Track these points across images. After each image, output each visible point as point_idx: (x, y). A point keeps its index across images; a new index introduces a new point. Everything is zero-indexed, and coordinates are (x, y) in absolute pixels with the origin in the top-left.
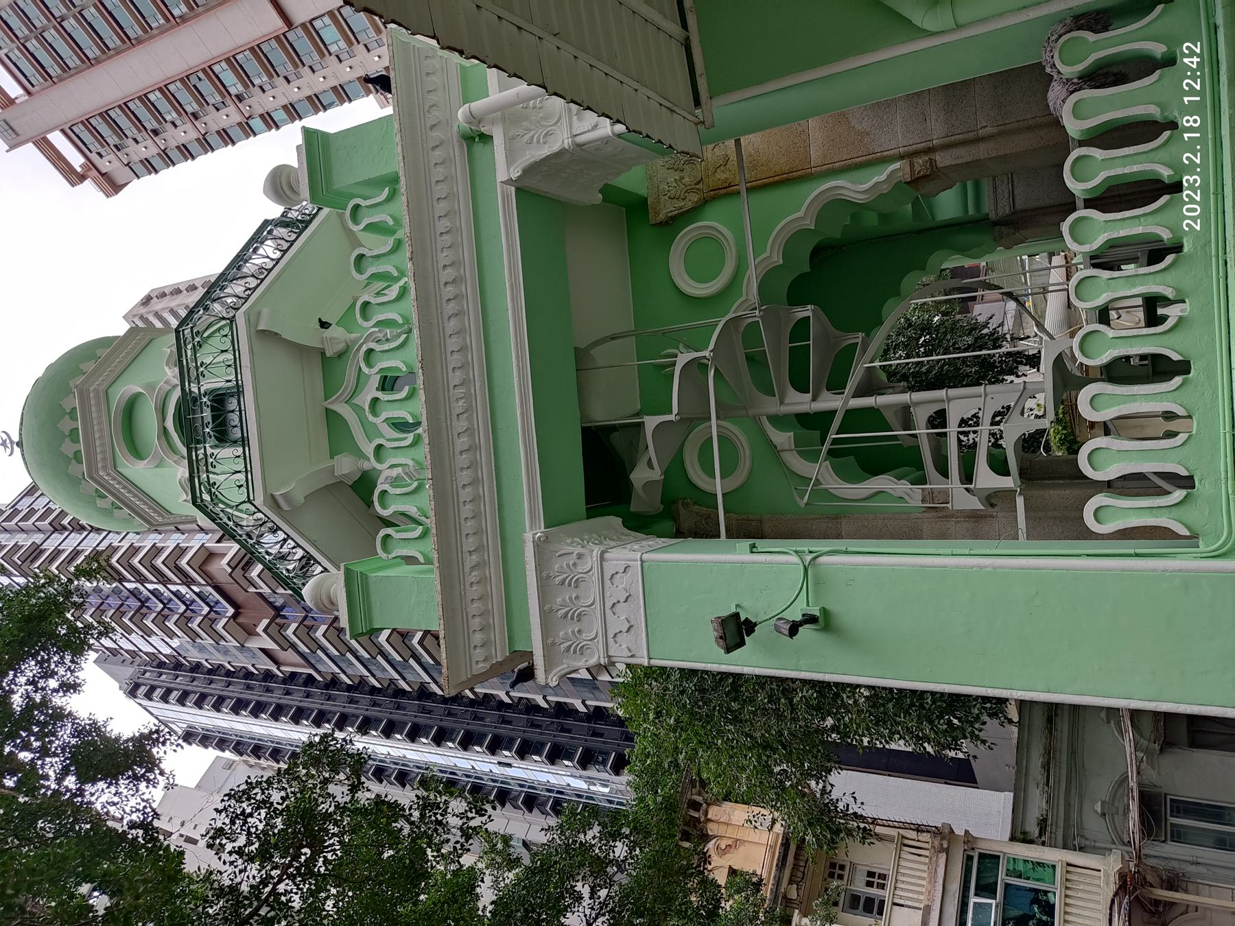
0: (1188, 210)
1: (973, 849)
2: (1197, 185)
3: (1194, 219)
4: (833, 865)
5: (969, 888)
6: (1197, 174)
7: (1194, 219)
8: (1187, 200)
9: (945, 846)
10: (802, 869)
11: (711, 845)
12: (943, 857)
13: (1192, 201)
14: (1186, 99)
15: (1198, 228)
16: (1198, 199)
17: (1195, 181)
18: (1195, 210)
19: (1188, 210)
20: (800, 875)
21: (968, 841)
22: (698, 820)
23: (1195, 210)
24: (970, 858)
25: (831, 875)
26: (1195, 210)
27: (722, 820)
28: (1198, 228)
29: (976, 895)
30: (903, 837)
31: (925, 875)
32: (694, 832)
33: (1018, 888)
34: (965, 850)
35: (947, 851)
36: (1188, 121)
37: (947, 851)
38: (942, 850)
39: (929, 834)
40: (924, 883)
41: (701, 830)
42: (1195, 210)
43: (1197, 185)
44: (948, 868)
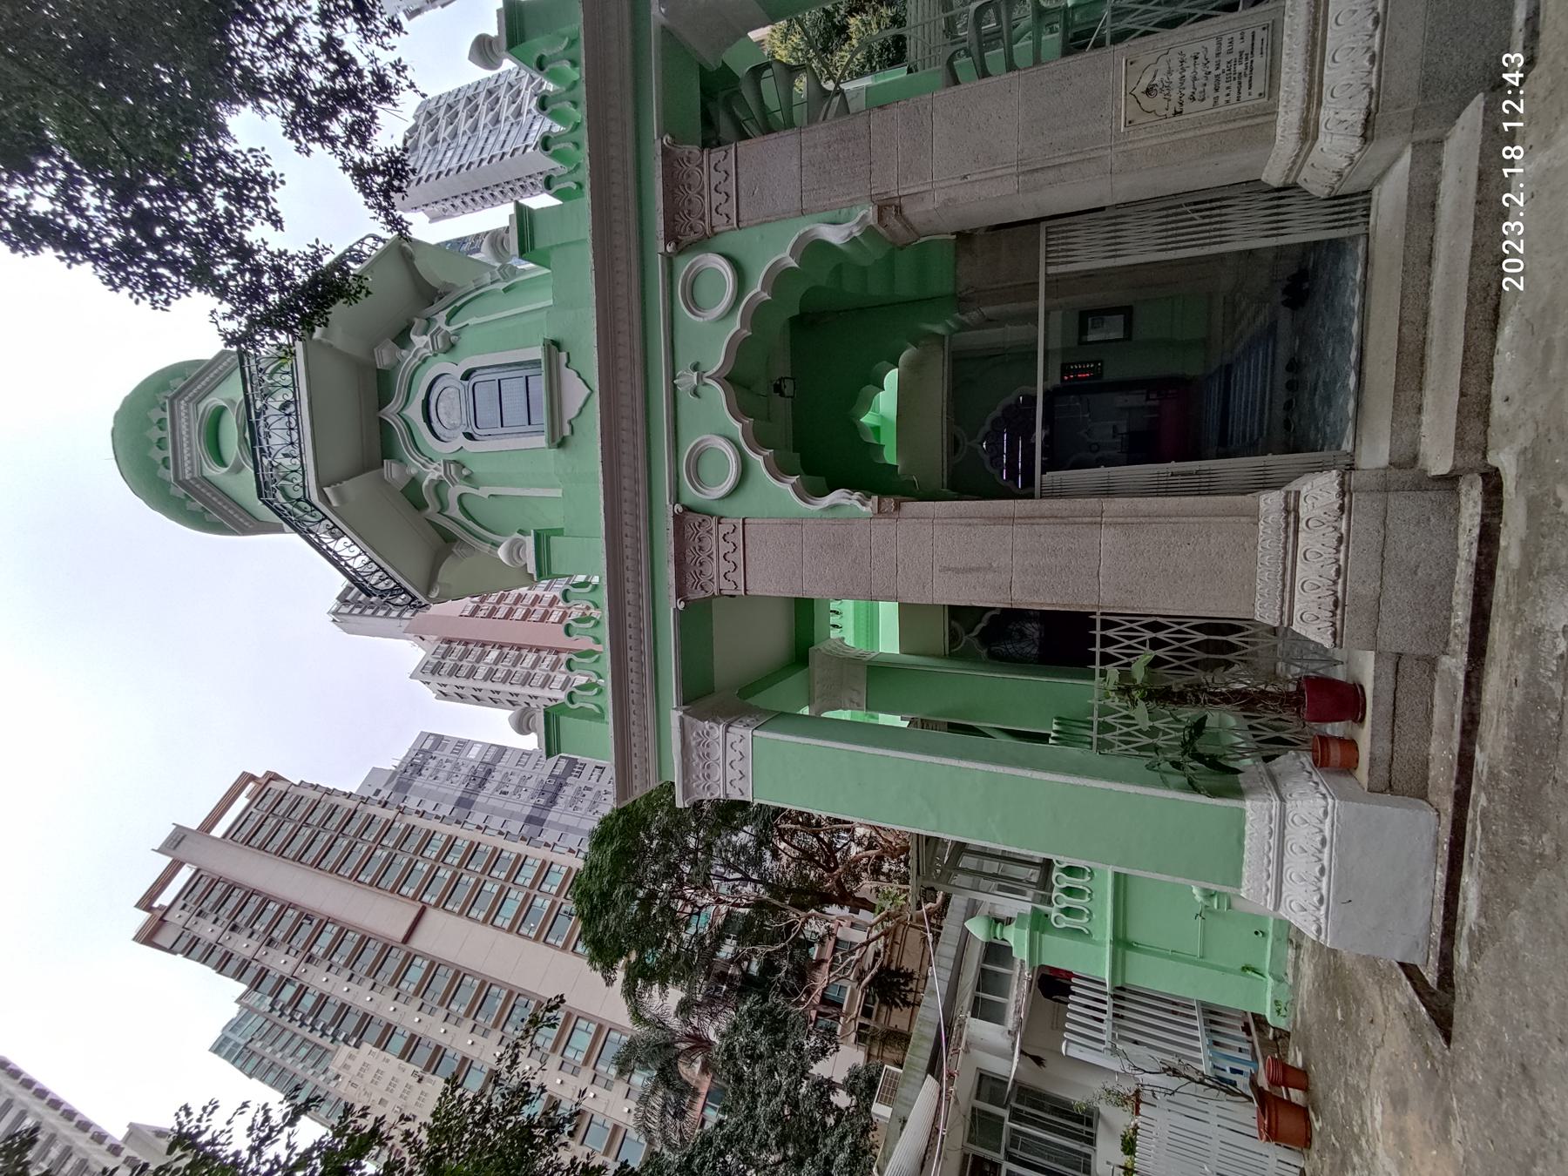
0: (1508, 265)
2: (1520, 233)
3: (1516, 276)
6: (1519, 219)
7: (1516, 276)
8: (1507, 252)
13: (1514, 254)
14: (1506, 125)
15: (1521, 288)
16: (1521, 251)
17: (1518, 228)
18: (1517, 265)
19: (1508, 265)
23: (1518, 265)
26: (1518, 265)
28: (1521, 288)
36: (1508, 153)
42: (1517, 265)
43: (1520, 233)
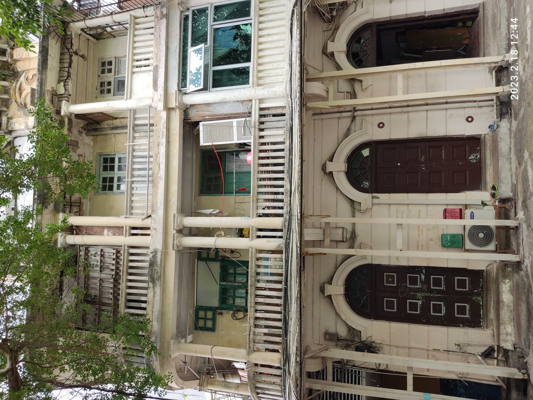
1: (189, 9)
4: (103, 64)
5: (187, 43)
9: (165, 12)
10: (67, 69)
11: (22, 79)
12: (164, 21)
20: (66, 74)
21: (182, 2)
22: (7, 62)
24: (186, 18)
25: (103, 72)
27: (24, 57)
29: (192, 46)
30: (136, 18)
31: (152, 43)
32: (6, 72)
33: (224, 30)
34: (182, 12)
35: (167, 16)
37: (167, 16)
38: (163, 16)
39: (152, 7)
40: (151, 49)
41: (13, 70)
44: (170, 30)
